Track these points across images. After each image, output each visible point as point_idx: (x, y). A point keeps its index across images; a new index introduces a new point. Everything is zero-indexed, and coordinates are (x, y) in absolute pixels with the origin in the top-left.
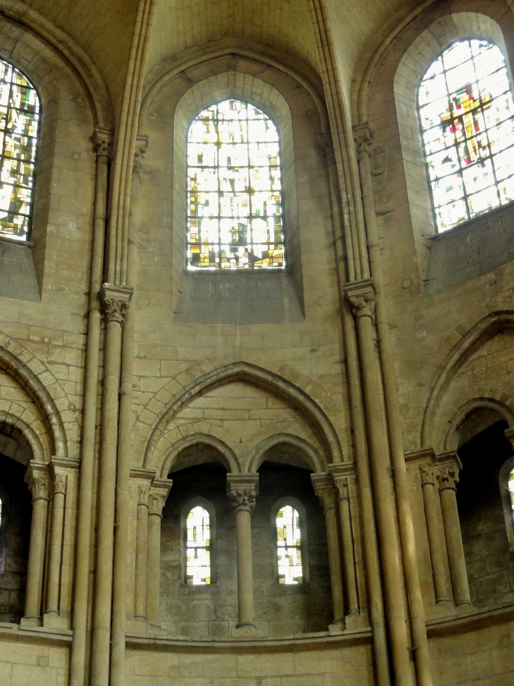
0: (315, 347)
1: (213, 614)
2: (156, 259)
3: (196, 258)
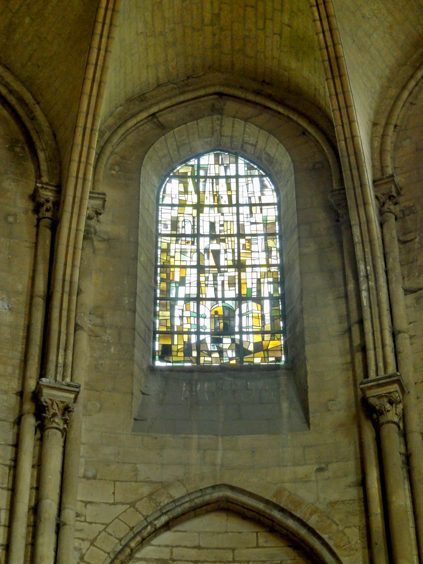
0: (323, 466)
2: (112, 350)
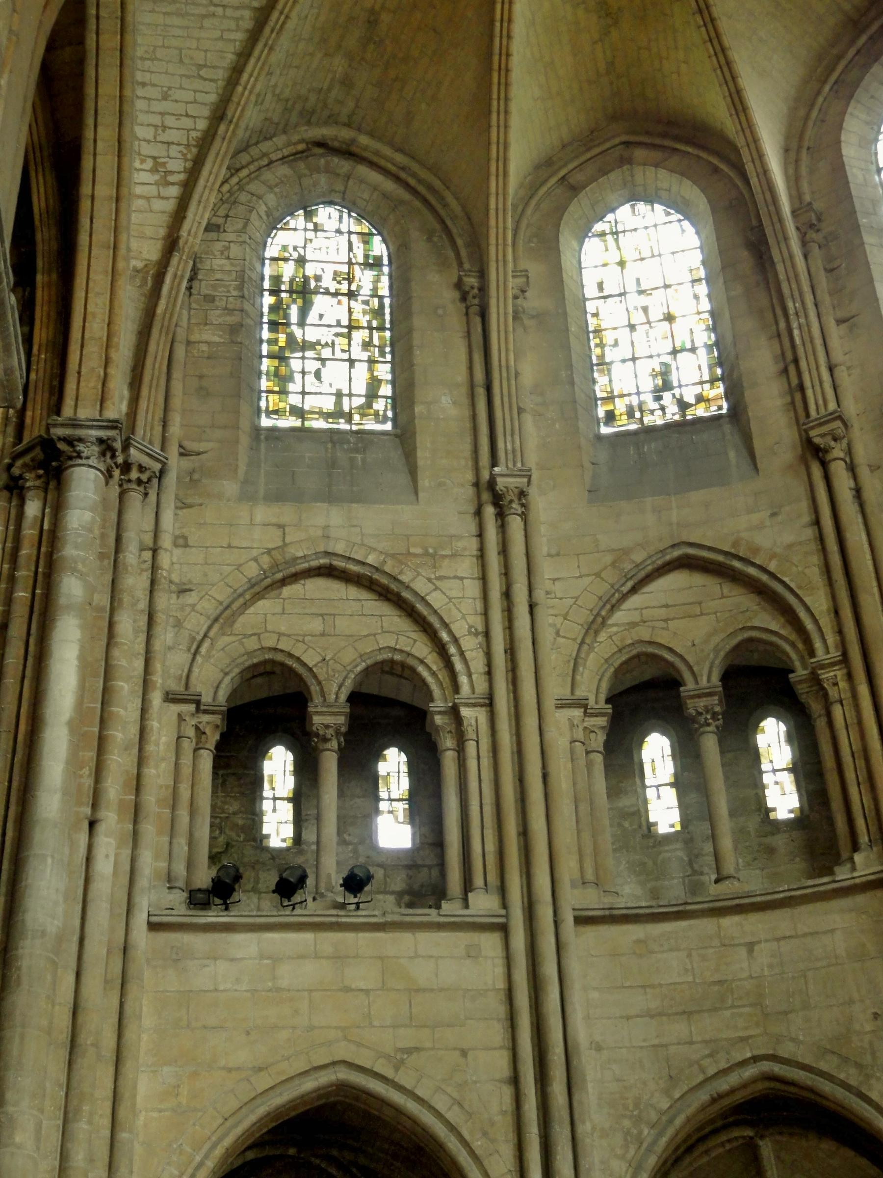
0: (775, 510)
1: (688, 868)
2: (557, 426)
3: (610, 417)
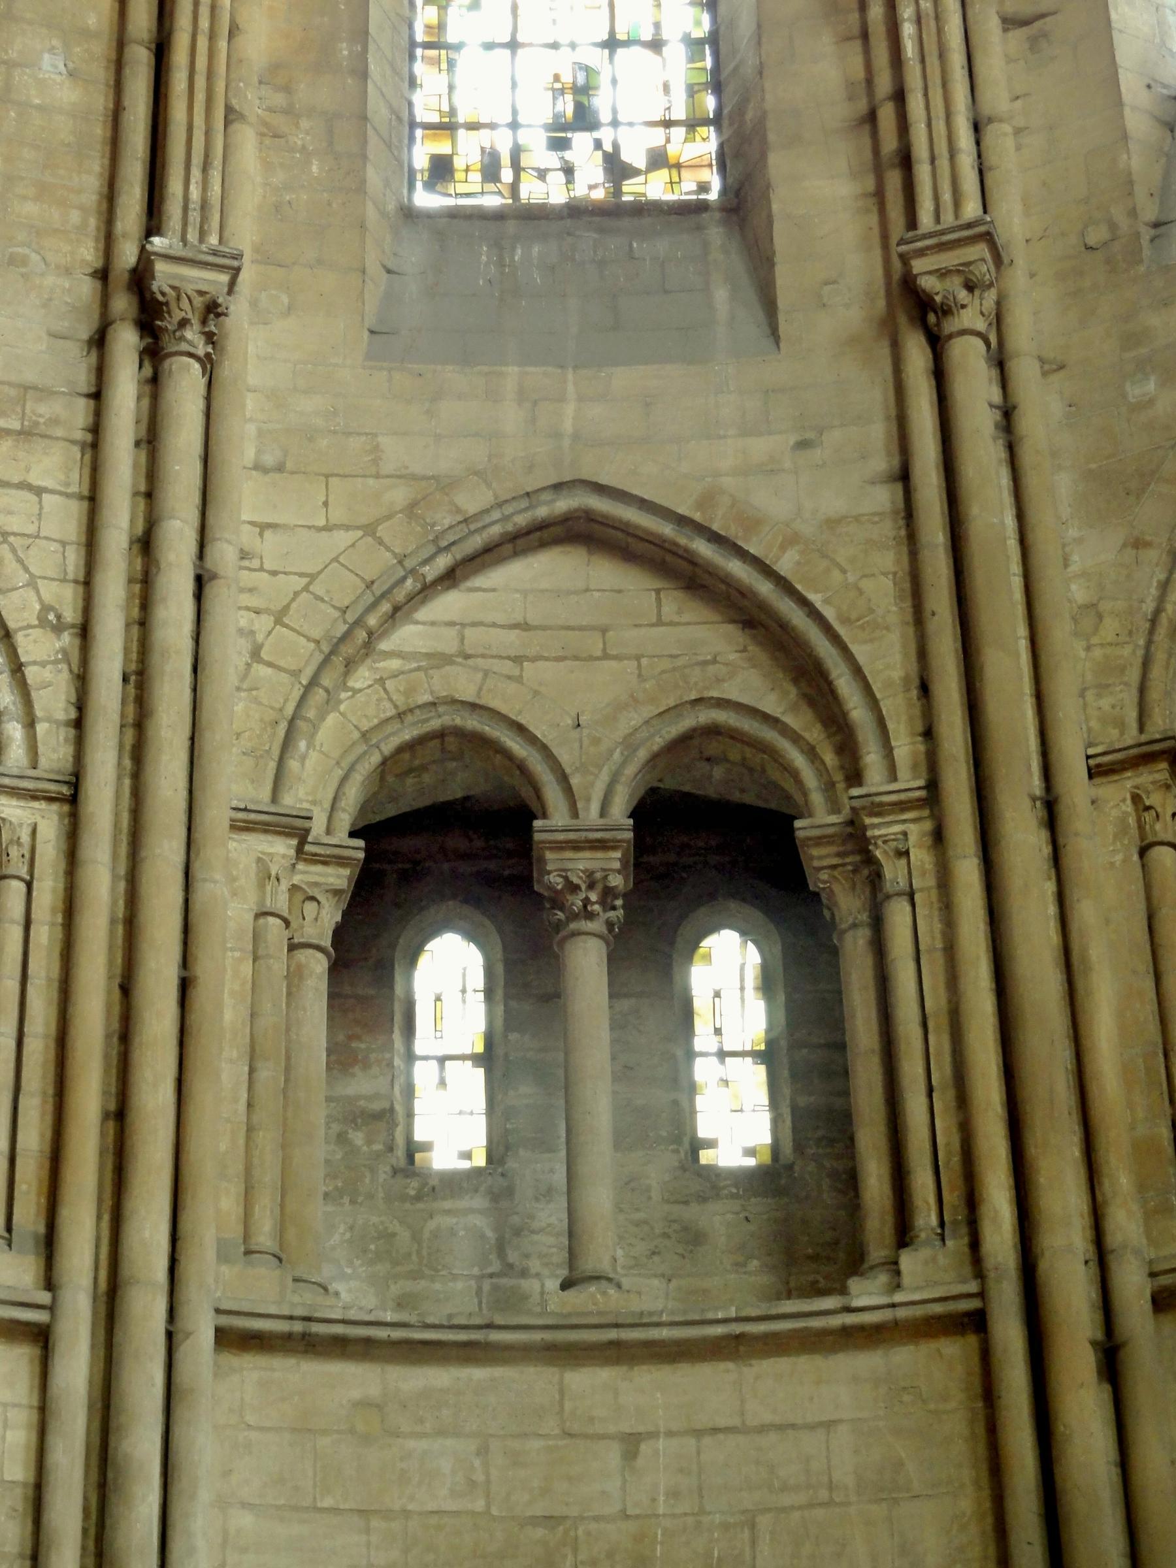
0: (810, 435)
1: (493, 1257)
2: (314, 169)
3: (442, 169)
